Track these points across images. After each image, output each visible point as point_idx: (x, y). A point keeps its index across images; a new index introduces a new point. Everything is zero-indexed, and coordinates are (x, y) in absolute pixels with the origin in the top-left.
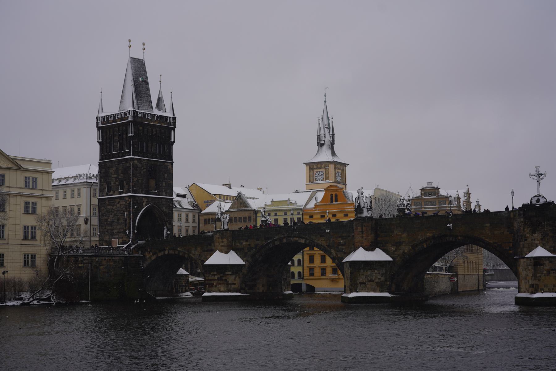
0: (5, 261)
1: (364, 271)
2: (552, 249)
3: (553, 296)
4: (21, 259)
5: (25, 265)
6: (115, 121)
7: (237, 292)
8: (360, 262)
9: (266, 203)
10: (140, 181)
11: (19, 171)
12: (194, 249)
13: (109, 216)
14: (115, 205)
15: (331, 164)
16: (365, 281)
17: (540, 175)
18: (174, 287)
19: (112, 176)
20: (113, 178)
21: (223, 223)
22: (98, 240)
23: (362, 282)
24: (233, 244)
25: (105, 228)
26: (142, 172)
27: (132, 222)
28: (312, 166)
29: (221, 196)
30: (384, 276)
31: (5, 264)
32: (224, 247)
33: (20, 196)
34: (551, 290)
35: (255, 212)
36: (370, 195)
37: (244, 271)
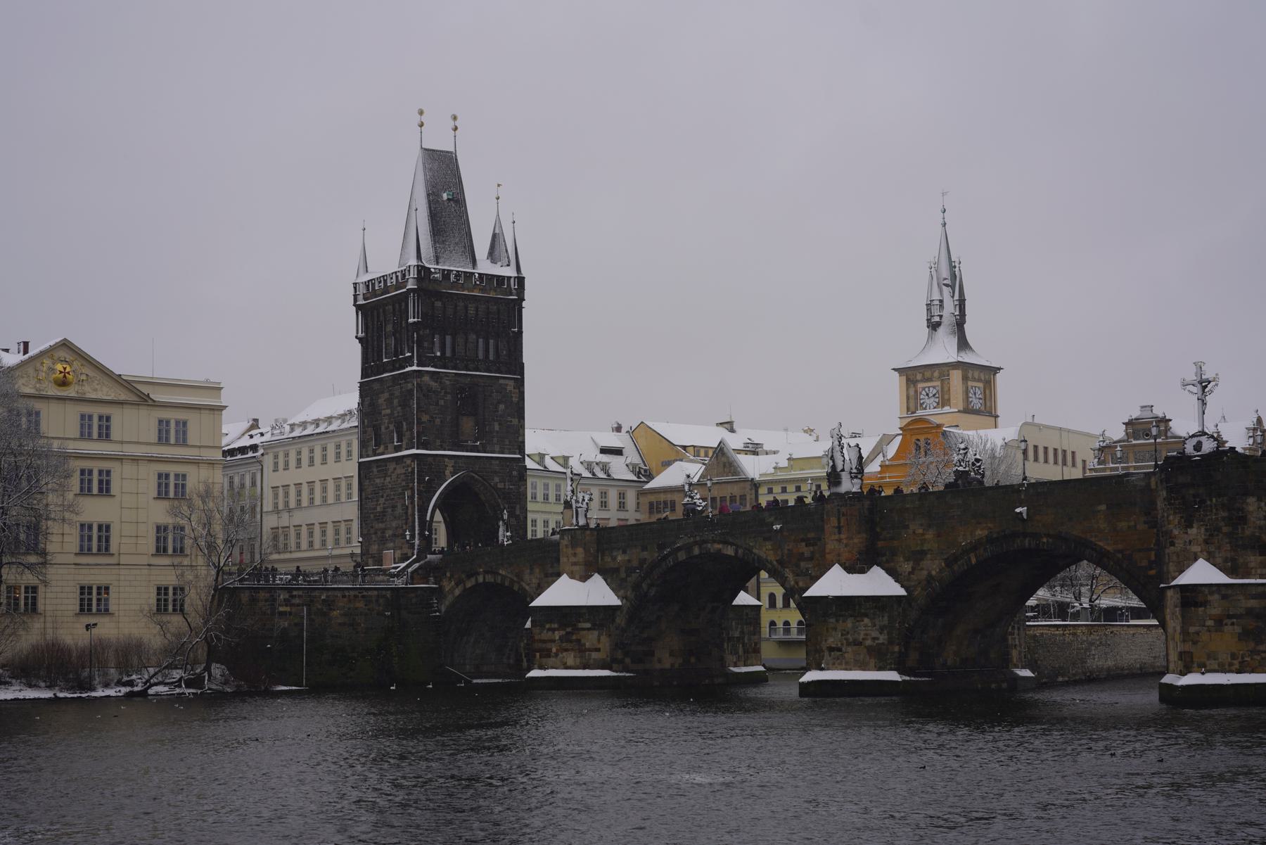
1: (837, 621)
2: (1229, 564)
3: (1229, 683)
4: (149, 598)
5: (82, 610)
6: (386, 290)
7: (603, 668)
8: (885, 599)
9: (777, 463)
10: (438, 421)
11: (146, 407)
12: (528, 571)
13: (377, 501)
15: (953, 369)
17: (1204, 385)
18: (523, 655)
19: (383, 412)
22: (360, 552)
24: (600, 558)
26: (443, 401)
27: (418, 512)
28: (912, 376)
29: (699, 451)
30: (885, 632)
31: (112, 608)
32: (578, 567)
35: (755, 485)
36: (1006, 441)
37: (620, 620)
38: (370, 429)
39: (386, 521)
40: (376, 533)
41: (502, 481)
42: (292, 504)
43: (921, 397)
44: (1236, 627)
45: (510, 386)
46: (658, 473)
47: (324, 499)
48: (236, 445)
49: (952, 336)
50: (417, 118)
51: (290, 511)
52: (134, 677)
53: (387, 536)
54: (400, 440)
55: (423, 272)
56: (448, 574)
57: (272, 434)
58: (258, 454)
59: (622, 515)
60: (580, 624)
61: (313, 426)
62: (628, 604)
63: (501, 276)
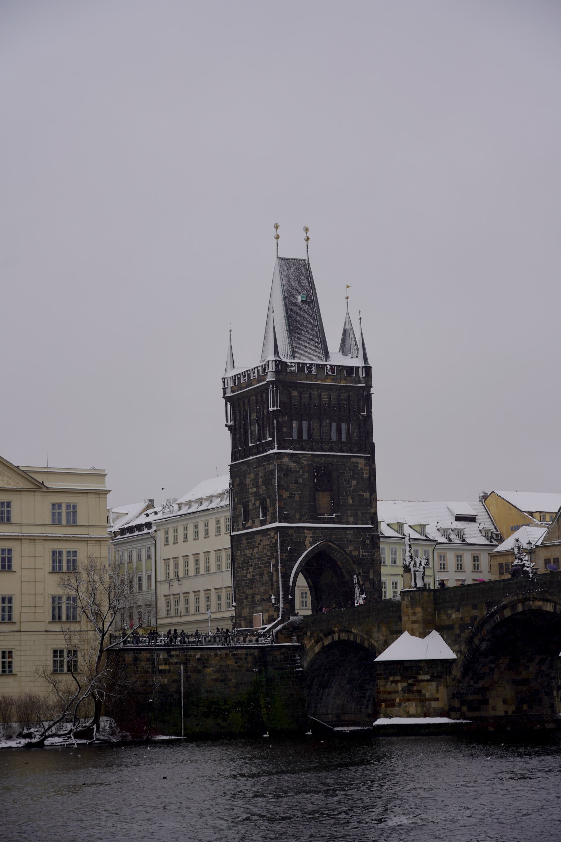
0: (14, 664)
6: (249, 384)
7: (442, 715)
10: (297, 498)
11: (40, 494)
12: (376, 629)
13: (248, 569)
14: (256, 547)
19: (251, 491)
20: (251, 494)
25: (244, 593)
26: (301, 479)
29: (544, 517)
31: (15, 669)
33: (42, 541)
37: (456, 672)
38: (240, 506)
39: (255, 587)
40: (247, 598)
42: (181, 574)
45: (361, 464)
46: (508, 537)
47: (208, 568)
48: (133, 524)
51: (179, 580)
52: (32, 730)
53: (256, 600)
54: (265, 515)
56: (309, 634)
57: (163, 513)
58: (152, 530)
59: (461, 576)
61: (197, 504)
62: (463, 657)
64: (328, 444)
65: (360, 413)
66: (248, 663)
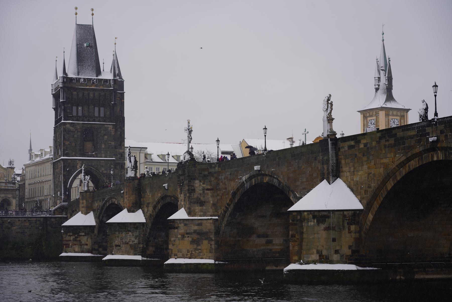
1: (119, 233)
3: (184, 263)
7: (88, 252)
10: (73, 144)
15: (381, 111)
16: (120, 243)
21: (84, 184)
23: (117, 244)
30: (137, 238)
34: (185, 256)
37: (96, 232)
41: (106, 170)
43: (369, 125)
44: (189, 238)
45: (110, 128)
49: (384, 95)
50: (75, 11)
55: (67, 80)
60: (80, 233)
62: (98, 225)
63: (106, 79)
64: (92, 118)
65: (111, 102)
66: (37, 224)
